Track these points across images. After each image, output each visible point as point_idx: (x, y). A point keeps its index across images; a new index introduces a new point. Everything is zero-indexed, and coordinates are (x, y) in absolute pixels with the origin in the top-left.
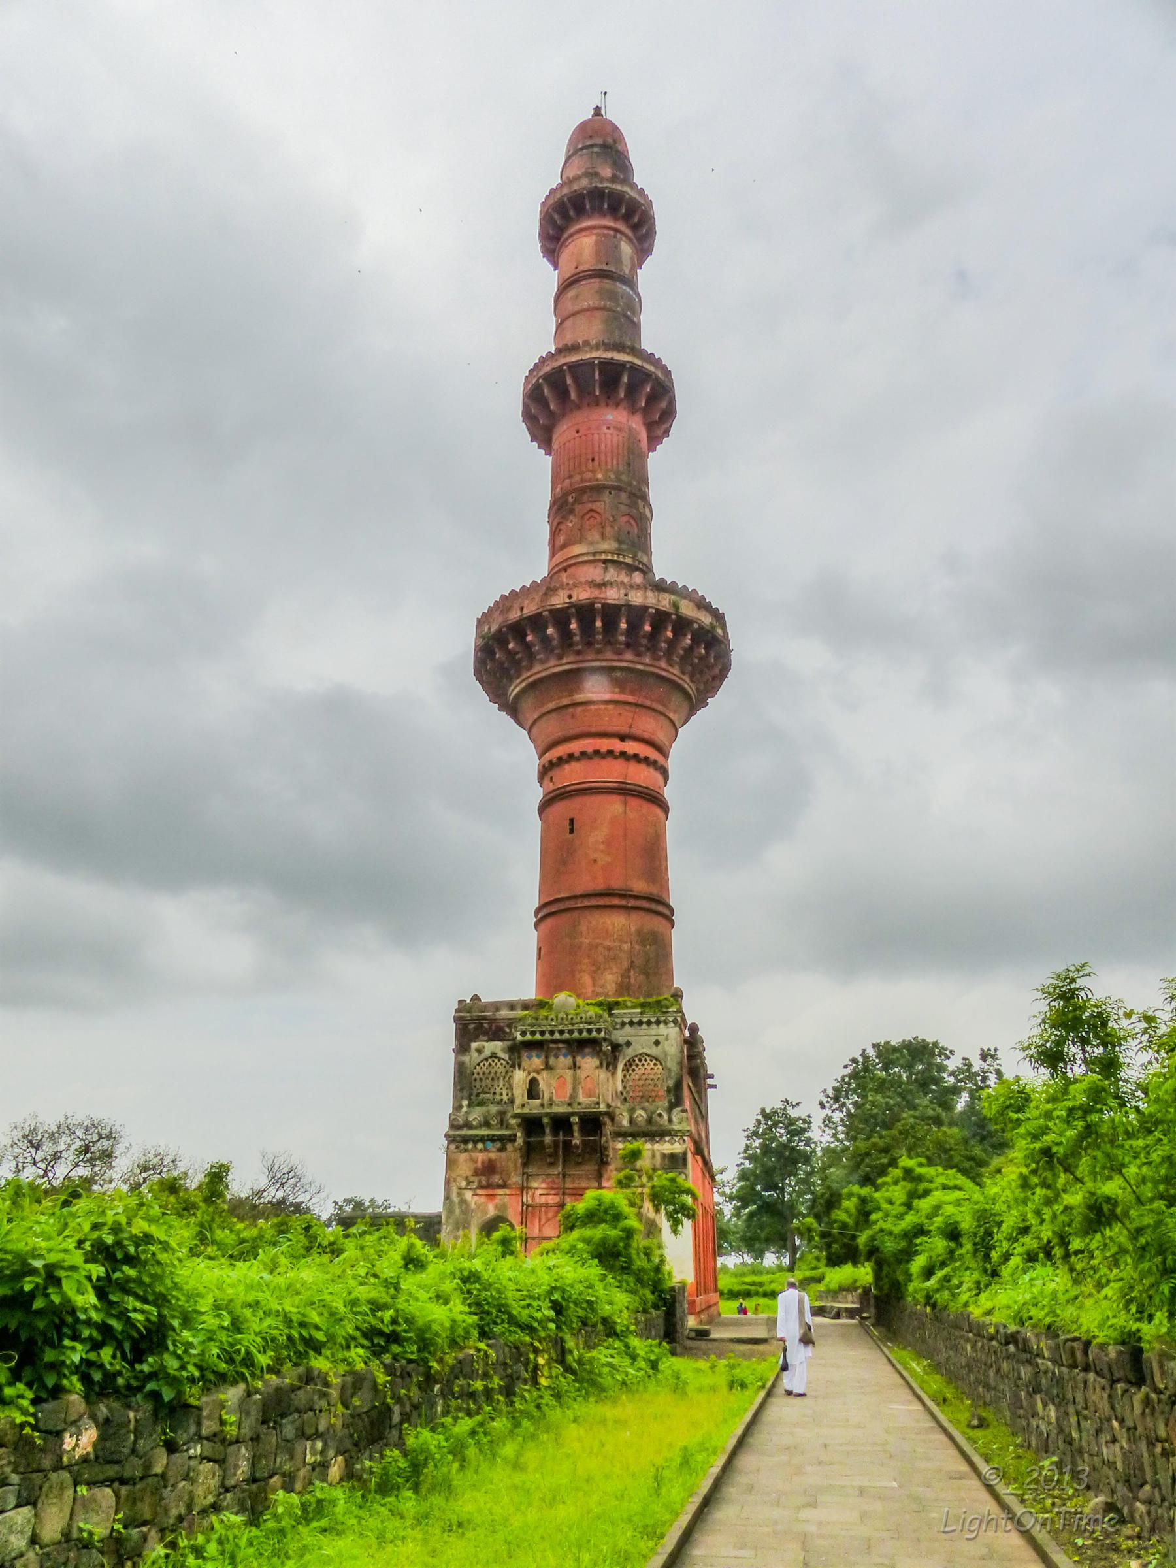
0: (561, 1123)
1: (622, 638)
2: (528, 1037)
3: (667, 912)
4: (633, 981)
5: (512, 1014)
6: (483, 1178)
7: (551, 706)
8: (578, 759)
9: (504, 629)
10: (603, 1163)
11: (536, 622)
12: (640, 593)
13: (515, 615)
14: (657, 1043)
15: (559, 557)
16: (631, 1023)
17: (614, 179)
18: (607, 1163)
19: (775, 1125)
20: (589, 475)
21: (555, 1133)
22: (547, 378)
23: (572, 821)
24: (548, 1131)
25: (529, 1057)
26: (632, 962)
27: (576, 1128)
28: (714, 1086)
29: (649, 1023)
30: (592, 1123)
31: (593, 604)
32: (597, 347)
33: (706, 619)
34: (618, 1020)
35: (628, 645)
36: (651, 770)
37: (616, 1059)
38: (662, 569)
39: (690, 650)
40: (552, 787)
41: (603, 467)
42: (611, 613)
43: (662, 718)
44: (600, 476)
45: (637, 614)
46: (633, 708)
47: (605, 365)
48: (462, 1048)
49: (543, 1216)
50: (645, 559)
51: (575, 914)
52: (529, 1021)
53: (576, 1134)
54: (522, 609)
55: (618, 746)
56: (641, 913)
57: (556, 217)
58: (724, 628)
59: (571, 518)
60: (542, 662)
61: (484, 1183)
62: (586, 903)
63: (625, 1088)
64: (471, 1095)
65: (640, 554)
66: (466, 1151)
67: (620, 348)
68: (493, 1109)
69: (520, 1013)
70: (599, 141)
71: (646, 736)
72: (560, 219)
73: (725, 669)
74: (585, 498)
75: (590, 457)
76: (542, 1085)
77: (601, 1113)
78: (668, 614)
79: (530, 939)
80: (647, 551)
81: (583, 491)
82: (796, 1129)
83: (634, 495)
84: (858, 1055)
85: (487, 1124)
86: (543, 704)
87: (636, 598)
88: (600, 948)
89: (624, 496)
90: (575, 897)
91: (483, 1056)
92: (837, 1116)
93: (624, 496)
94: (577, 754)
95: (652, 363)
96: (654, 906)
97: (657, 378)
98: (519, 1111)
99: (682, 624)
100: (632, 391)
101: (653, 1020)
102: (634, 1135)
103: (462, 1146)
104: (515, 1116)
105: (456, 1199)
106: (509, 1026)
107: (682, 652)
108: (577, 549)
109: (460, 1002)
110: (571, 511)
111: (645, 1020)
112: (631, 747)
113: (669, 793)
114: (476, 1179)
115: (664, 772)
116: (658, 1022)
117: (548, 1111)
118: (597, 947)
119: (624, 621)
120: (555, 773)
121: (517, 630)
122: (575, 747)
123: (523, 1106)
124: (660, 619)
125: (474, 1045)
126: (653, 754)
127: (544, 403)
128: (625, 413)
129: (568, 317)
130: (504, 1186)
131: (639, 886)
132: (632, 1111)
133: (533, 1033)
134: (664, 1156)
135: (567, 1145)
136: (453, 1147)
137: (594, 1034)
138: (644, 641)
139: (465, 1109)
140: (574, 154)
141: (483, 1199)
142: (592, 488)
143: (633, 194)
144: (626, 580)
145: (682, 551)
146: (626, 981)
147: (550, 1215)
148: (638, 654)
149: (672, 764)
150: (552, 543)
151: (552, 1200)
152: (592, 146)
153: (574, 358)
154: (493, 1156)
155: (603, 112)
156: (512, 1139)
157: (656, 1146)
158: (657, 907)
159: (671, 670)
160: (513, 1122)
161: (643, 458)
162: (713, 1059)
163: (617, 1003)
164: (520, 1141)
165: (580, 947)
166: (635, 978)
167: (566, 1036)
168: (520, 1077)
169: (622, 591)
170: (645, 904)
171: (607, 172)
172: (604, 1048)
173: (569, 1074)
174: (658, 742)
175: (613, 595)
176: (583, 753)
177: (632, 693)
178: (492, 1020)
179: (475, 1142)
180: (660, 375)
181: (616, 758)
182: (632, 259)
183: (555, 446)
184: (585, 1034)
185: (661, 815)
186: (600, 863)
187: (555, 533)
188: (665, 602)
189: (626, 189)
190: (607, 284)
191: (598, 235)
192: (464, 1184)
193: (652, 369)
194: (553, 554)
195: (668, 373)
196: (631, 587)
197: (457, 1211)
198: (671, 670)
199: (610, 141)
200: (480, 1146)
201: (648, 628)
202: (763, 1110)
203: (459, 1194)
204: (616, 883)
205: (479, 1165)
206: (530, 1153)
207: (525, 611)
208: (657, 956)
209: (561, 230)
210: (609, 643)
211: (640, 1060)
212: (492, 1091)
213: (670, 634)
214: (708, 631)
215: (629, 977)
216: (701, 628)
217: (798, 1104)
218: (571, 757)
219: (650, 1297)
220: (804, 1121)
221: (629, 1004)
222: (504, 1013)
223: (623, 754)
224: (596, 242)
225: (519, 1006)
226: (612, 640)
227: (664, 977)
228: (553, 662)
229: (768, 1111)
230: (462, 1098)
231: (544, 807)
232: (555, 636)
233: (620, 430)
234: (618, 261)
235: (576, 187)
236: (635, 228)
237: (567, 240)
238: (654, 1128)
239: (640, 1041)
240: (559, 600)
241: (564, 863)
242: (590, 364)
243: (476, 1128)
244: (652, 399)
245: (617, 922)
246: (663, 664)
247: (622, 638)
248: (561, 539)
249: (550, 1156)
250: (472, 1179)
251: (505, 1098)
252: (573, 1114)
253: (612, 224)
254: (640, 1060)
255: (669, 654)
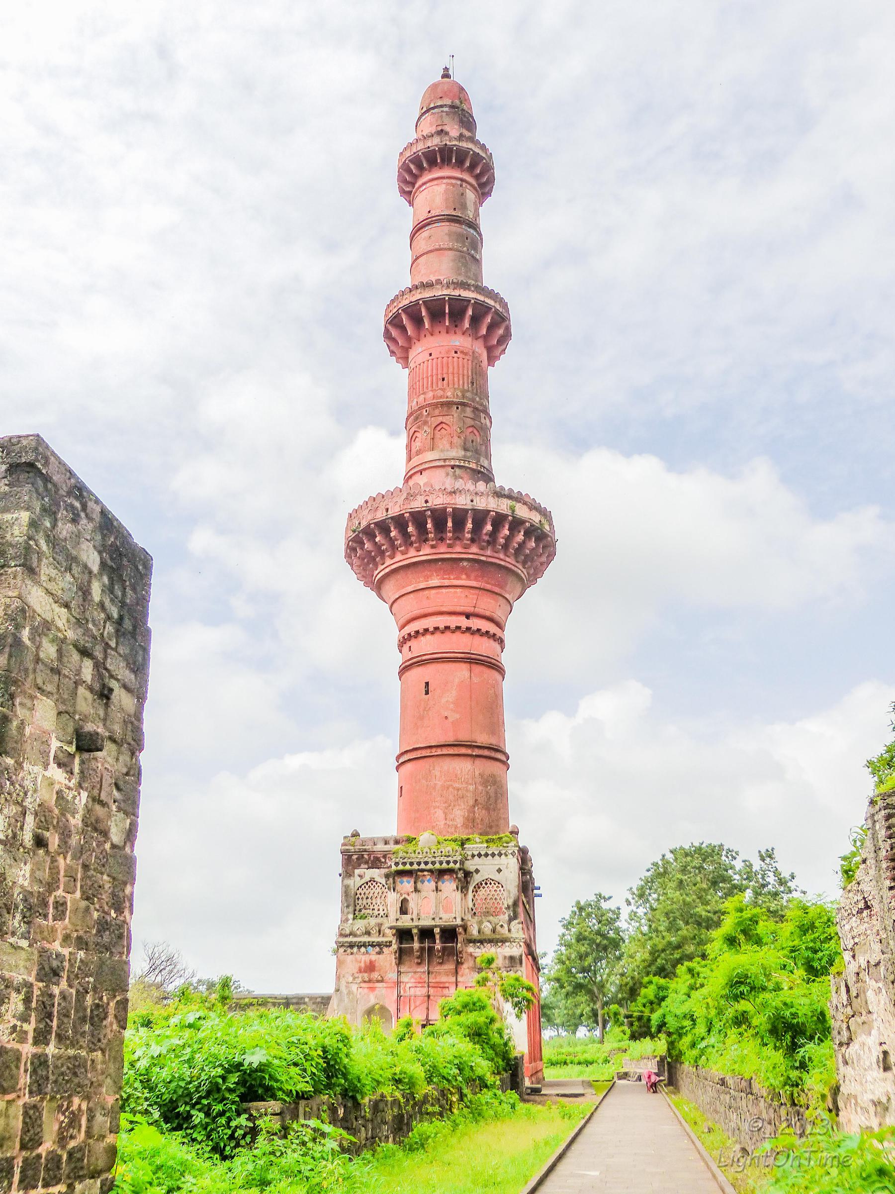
0: (426, 933)
1: (468, 536)
2: (401, 867)
3: (504, 758)
4: (477, 815)
5: (387, 848)
6: (366, 975)
7: (410, 589)
8: (432, 633)
9: (373, 526)
10: (459, 964)
11: (400, 522)
12: (484, 499)
13: (380, 515)
14: (499, 871)
15: (416, 461)
16: (480, 855)
17: (461, 137)
18: (462, 964)
19: (589, 915)
20: (440, 393)
21: (421, 940)
22: (406, 310)
23: (427, 684)
24: (416, 938)
25: (402, 883)
26: (476, 800)
27: (437, 937)
28: (540, 896)
29: (493, 855)
30: (450, 934)
31: (446, 508)
32: (448, 287)
33: (536, 518)
34: (470, 853)
35: (473, 540)
36: (491, 641)
37: (468, 883)
38: (500, 481)
39: (522, 545)
40: (410, 655)
41: (451, 386)
42: (459, 517)
43: (500, 598)
44: (449, 394)
45: (480, 517)
46: (477, 591)
47: (453, 300)
48: (347, 874)
49: (412, 1001)
50: (486, 464)
51: (431, 760)
52: (401, 854)
53: (438, 941)
54: (387, 510)
55: (463, 622)
56: (484, 760)
57: (412, 167)
58: (551, 524)
59: (426, 428)
60: (403, 553)
61: (367, 979)
62: (439, 752)
63: (474, 905)
64: (355, 910)
65: (482, 459)
66: (352, 954)
67: (464, 286)
68: (373, 922)
69: (392, 847)
70: (448, 102)
71: (488, 614)
72: (415, 169)
73: (551, 556)
74: (437, 412)
75: (440, 377)
76: (411, 905)
77: (457, 926)
78: (507, 516)
79: (394, 780)
80: (488, 456)
81: (435, 405)
82: (609, 920)
83: (477, 409)
84: (658, 859)
85: (368, 933)
86: (403, 587)
87: (481, 504)
88: (451, 789)
89: (469, 410)
90: (430, 747)
91: (363, 881)
92: (641, 911)
93: (469, 410)
94: (431, 629)
95: (491, 298)
96: (493, 754)
97: (497, 312)
98: (394, 924)
99: (517, 523)
100: (476, 320)
101: (496, 853)
102: (481, 942)
103: (349, 950)
104: (391, 928)
105: (343, 989)
106: (385, 857)
107: (516, 546)
108: (430, 456)
109: (345, 837)
110: (426, 423)
111: (490, 852)
112: (476, 623)
113: (506, 659)
114: (360, 975)
115: (501, 641)
116: (500, 855)
117: (416, 924)
118: (448, 788)
119: (470, 521)
120: (413, 643)
121: (383, 527)
122: (430, 623)
123: (397, 920)
124: (499, 520)
125: (357, 872)
126: (493, 629)
127: (403, 329)
128: (470, 339)
129: (423, 254)
130: (382, 981)
131: (482, 738)
132: (480, 923)
133: (404, 864)
134: (505, 957)
135: (431, 949)
136: (341, 950)
137: (452, 865)
138: (486, 538)
139: (351, 921)
140: (427, 111)
141: (366, 991)
142: (443, 404)
143: (477, 150)
144: (472, 488)
145: (520, 465)
146: (471, 815)
147: (418, 1003)
148: (482, 549)
149: (508, 635)
150: (409, 447)
151: (421, 991)
152: (441, 106)
153: (428, 294)
154: (374, 957)
155: (451, 72)
156: (389, 945)
157: (499, 950)
158: (494, 753)
159: (508, 559)
160: (388, 931)
161: (483, 375)
162: (539, 875)
163: (468, 839)
164: (395, 946)
165: (434, 788)
166: (480, 813)
167: (430, 866)
168: (393, 899)
169: (469, 498)
170: (486, 753)
171: (454, 130)
172: (459, 876)
173: (433, 895)
174: (498, 619)
175: (462, 502)
176: (436, 629)
177: (476, 580)
178: (370, 853)
179: (359, 947)
180: (498, 307)
181: (463, 632)
182: (475, 203)
183: (412, 365)
184: (444, 866)
185: (499, 677)
186: (450, 719)
187: (412, 438)
188: (503, 506)
189: (470, 146)
190: (455, 227)
191: (448, 184)
192: (351, 979)
193: (491, 302)
194: (410, 459)
195: (505, 306)
196: (476, 494)
197: (346, 1000)
198: (508, 559)
199: (457, 102)
200: (363, 949)
201: (489, 527)
202: (578, 903)
203: (347, 987)
204: (464, 736)
205: (363, 965)
206: (402, 955)
207: (389, 512)
208: (496, 793)
209: (416, 177)
210: (458, 538)
211: (486, 884)
212: (372, 907)
213: (507, 532)
214: (538, 528)
215: (474, 812)
216: (532, 525)
217: (610, 898)
218: (426, 630)
219: (501, 1063)
220: (613, 912)
221: (478, 840)
222: (381, 847)
223: (468, 629)
224: (446, 191)
225: (392, 842)
226: (460, 536)
227: (502, 811)
228: (412, 552)
229: (582, 903)
230: (348, 913)
231: (404, 670)
232: (414, 533)
233: (466, 354)
234: (464, 206)
235: (429, 143)
236: (477, 177)
237: (420, 186)
238: (498, 937)
239: (485, 868)
240: (418, 504)
241: (421, 718)
242: (440, 301)
243: (360, 936)
244: (492, 327)
245: (464, 767)
246: (502, 556)
247: (468, 536)
248: (417, 445)
249: (418, 958)
250: (357, 975)
251: (382, 913)
252: (436, 926)
253: (460, 176)
254: (486, 884)
255: (506, 547)
